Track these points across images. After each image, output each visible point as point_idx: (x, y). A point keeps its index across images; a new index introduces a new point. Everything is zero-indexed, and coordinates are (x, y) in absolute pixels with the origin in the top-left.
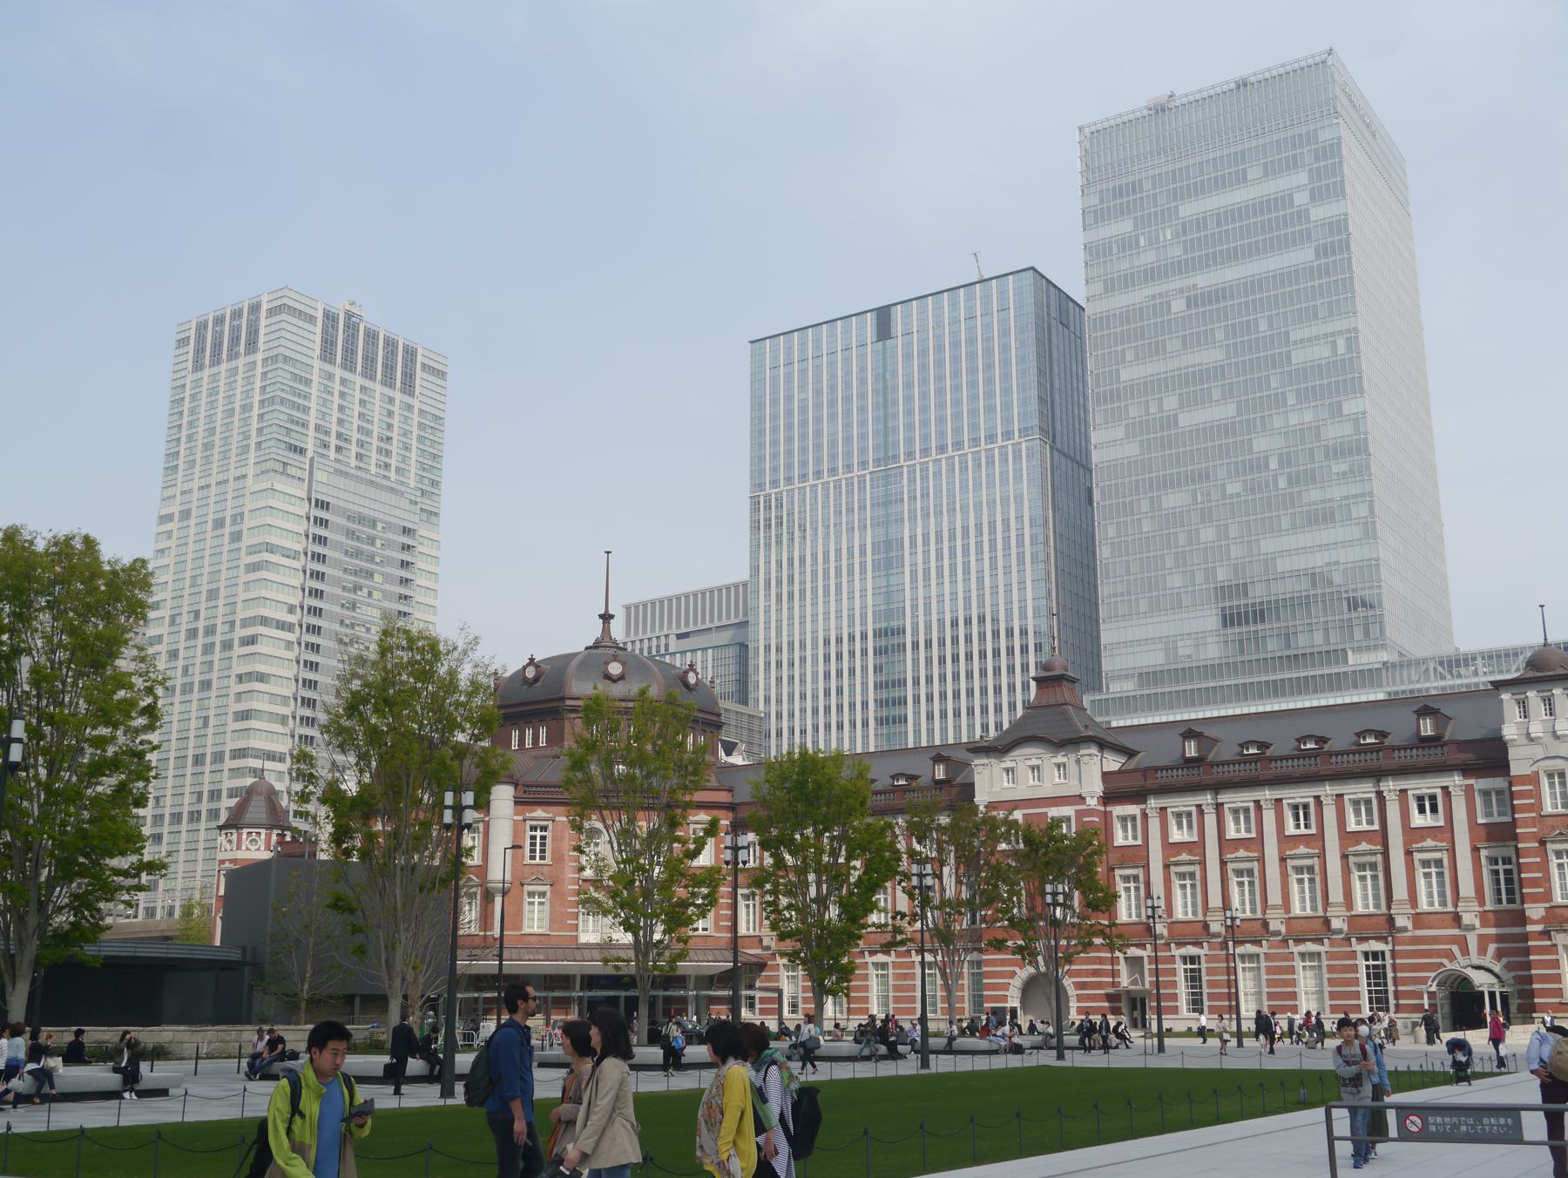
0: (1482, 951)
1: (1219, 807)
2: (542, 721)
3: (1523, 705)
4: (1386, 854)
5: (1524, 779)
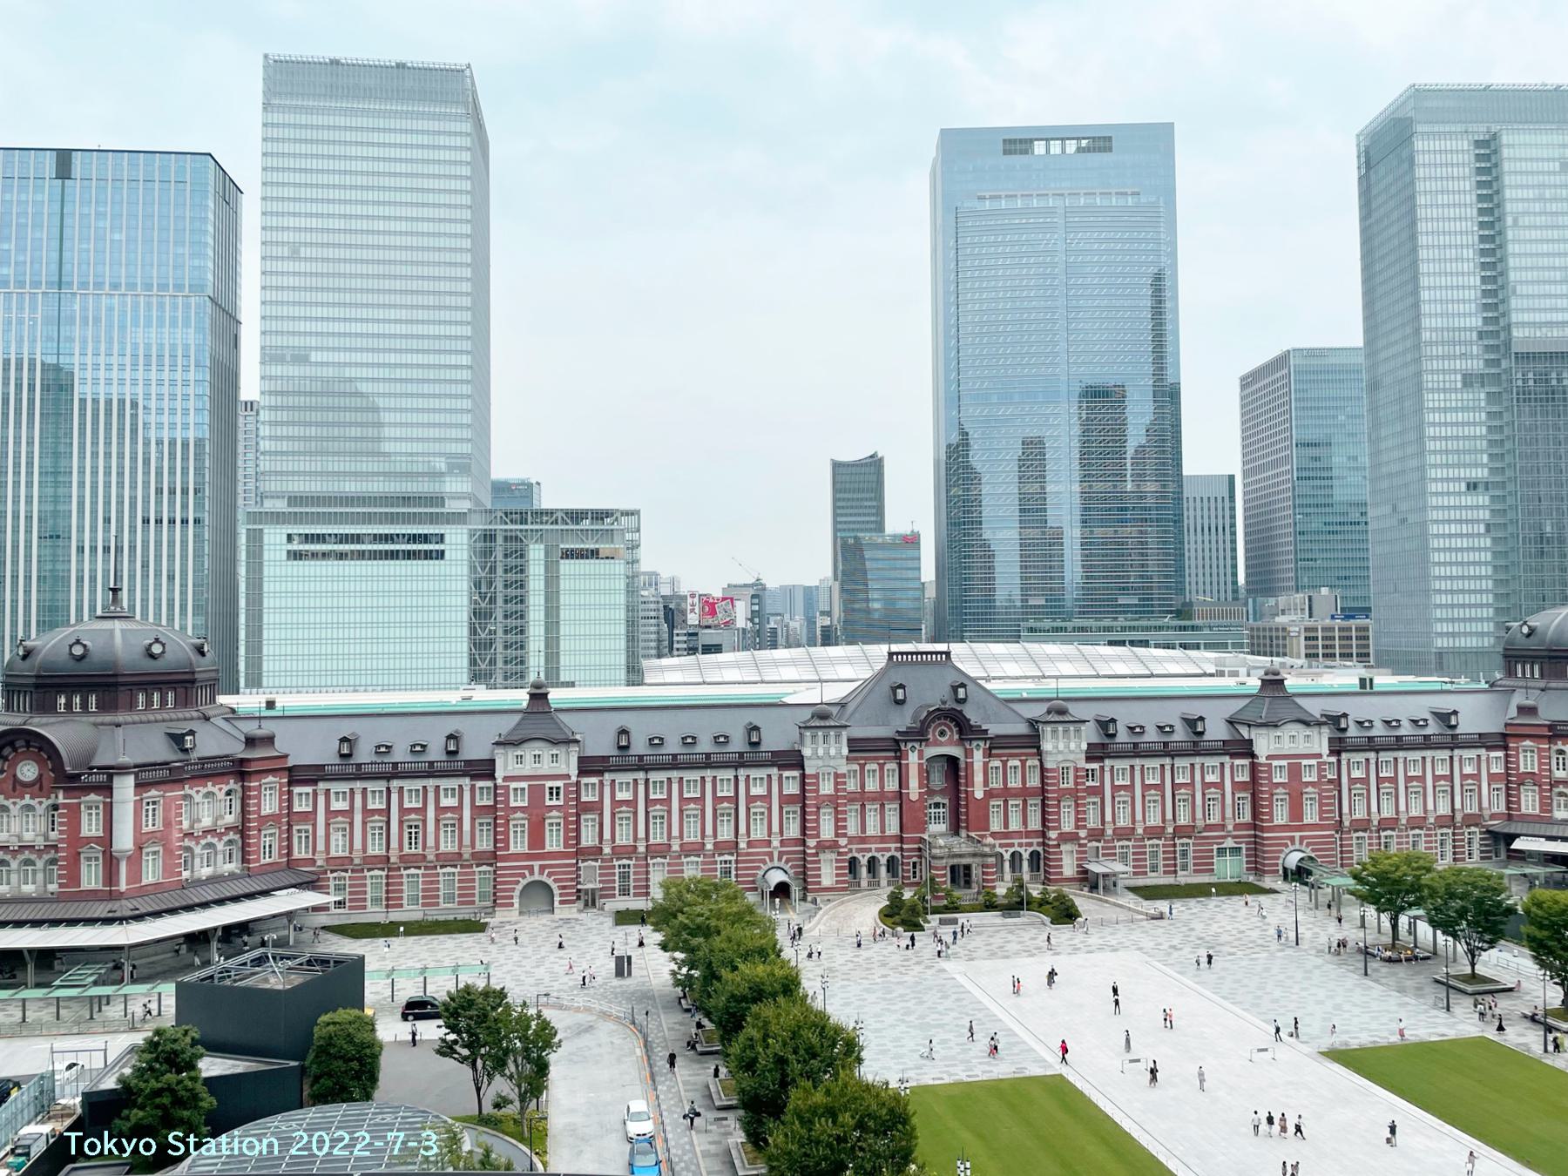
0: (780, 859)
1: (647, 781)
2: (92, 692)
4: (737, 810)
5: (812, 776)
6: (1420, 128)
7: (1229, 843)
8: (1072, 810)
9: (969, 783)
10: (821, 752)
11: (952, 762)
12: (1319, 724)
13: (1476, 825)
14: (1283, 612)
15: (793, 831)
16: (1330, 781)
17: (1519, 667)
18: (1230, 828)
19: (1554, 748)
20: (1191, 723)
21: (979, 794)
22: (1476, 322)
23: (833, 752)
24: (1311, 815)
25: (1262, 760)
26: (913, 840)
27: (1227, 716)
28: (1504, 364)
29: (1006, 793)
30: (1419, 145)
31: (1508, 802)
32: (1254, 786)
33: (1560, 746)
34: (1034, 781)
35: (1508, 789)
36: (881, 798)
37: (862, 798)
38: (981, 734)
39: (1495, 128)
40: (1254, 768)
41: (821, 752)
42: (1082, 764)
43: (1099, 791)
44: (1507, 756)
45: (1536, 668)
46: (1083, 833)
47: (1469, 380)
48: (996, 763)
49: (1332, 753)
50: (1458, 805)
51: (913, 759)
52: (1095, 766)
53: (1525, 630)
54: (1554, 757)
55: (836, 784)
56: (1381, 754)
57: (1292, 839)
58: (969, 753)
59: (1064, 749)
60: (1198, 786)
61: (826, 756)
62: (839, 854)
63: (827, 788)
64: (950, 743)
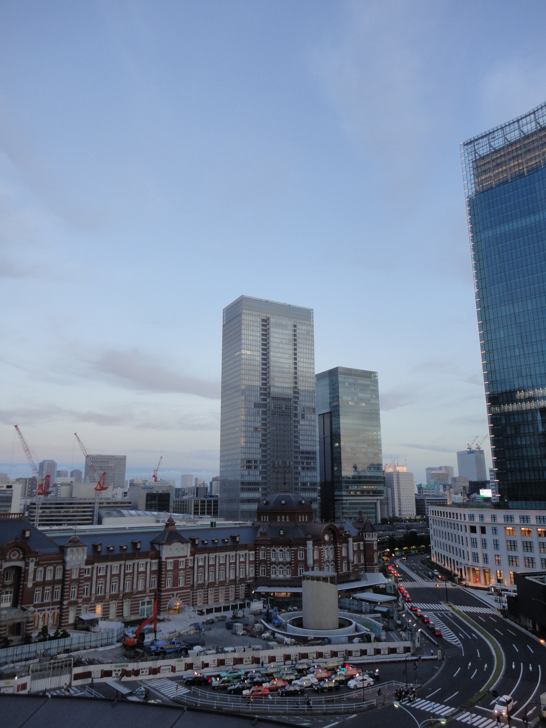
6: (244, 311)
7: (147, 599)
8: (76, 590)
9: (26, 579)
11: (18, 569)
12: (187, 542)
13: (244, 583)
16: (190, 567)
17: (262, 517)
18: (148, 591)
19: (272, 549)
20: (134, 544)
21: (30, 585)
24: (181, 585)
25: (163, 560)
27: (151, 540)
28: (268, 400)
29: (44, 583)
30: (244, 317)
31: (256, 572)
32: (160, 572)
33: (274, 548)
34: (59, 576)
35: (256, 567)
38: (36, 555)
40: (160, 564)
42: (84, 566)
43: (90, 579)
44: (256, 553)
45: (268, 517)
46: (80, 601)
47: (256, 405)
49: (191, 555)
50: (237, 575)
52: (90, 567)
53: (264, 502)
54: (272, 552)
56: (210, 554)
57: (173, 595)
58: (27, 565)
59: (76, 558)
60: (136, 573)
64: (18, 560)
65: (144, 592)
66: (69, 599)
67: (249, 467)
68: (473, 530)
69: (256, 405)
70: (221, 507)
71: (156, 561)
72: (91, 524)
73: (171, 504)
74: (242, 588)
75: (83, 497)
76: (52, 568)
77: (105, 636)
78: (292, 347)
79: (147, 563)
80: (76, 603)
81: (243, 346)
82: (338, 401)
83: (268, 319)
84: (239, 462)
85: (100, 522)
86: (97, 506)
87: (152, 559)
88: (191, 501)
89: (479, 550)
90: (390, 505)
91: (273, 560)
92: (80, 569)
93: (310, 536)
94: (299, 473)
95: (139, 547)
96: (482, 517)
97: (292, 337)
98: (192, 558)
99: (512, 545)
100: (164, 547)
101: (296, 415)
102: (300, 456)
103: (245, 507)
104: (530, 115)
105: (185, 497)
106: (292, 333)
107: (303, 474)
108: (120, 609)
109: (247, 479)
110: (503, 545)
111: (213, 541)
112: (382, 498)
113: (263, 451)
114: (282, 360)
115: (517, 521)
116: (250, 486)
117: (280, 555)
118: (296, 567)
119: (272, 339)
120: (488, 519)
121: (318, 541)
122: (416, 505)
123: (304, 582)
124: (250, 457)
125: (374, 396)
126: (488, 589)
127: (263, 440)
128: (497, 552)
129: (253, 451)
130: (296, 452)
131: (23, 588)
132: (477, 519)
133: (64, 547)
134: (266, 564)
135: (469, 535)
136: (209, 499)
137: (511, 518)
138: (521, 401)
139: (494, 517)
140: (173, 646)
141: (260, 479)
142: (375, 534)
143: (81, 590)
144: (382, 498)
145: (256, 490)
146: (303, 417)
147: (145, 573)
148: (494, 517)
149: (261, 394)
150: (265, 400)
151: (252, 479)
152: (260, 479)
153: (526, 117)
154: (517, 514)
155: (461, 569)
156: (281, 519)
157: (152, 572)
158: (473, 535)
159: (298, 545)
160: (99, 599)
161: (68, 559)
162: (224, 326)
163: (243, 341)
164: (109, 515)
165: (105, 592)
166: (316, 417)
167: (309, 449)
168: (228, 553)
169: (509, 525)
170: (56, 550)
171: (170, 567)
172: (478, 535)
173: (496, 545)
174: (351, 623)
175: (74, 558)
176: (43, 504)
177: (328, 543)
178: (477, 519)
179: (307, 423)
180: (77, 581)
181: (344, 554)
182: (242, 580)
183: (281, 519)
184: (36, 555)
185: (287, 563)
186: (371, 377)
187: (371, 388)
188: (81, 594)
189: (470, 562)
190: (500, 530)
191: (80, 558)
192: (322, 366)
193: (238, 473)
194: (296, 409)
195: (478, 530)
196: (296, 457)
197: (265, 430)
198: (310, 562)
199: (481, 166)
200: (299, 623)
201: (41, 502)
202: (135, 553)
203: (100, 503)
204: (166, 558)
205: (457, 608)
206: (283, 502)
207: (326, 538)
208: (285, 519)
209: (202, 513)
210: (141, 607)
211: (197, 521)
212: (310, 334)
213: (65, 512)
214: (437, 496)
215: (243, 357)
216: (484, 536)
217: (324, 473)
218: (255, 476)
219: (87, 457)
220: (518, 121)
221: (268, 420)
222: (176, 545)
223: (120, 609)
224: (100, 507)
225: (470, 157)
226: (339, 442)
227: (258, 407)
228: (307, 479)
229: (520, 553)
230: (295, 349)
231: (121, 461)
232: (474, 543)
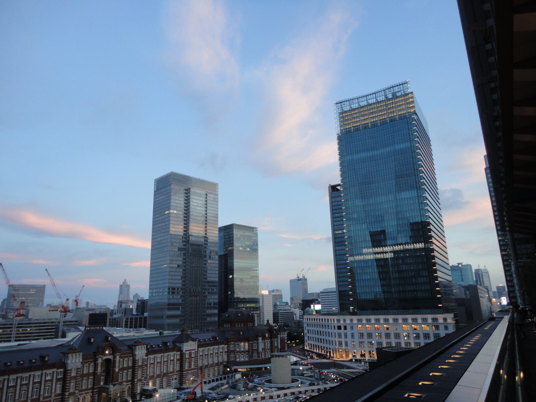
3: (72, 356)
7: (175, 377)
9: (114, 366)
10: (73, 361)
11: (108, 360)
14: (115, 314)
15: (59, 391)
21: (117, 370)
22: (182, 234)
23: (77, 361)
24: (193, 367)
25: (184, 352)
26: (97, 388)
28: (187, 246)
29: (123, 369)
32: (181, 360)
34: (130, 364)
35: (228, 354)
36: (88, 375)
37: (83, 376)
38: (120, 351)
39: (189, 187)
41: (73, 361)
46: (143, 378)
47: (180, 249)
48: (122, 360)
51: (100, 361)
53: (227, 315)
55: (77, 371)
58: (115, 357)
59: (140, 352)
61: (74, 362)
62: (76, 396)
63: (73, 374)
65: (173, 372)
66: (69, 391)
67: (173, 293)
68: (339, 328)
69: (180, 249)
70: (148, 322)
71: (179, 353)
72: (10, 341)
73: (108, 321)
74: (221, 367)
75: (37, 318)
76: (127, 359)
77: (172, 396)
78: (204, 209)
79: (53, 372)
80: (141, 380)
81: (172, 207)
82: (233, 246)
83: (189, 189)
84: (166, 289)
85: (64, 336)
86: (61, 324)
87: (58, 369)
88: (123, 319)
89: (343, 340)
90: (261, 317)
91: (238, 350)
92: (143, 359)
93: (260, 335)
94: (206, 296)
95: (46, 359)
96: (345, 320)
97: (204, 203)
98: (146, 358)
99: (362, 335)
100: (185, 344)
101: (205, 256)
102: (207, 284)
103: (169, 321)
104: (373, 94)
105: (115, 316)
106: (204, 199)
107: (208, 297)
108: (161, 383)
109: (172, 301)
110: (356, 336)
111: (205, 340)
112: (258, 312)
113: (183, 281)
114: (198, 218)
115: (364, 322)
116: (172, 306)
117: (244, 346)
118: (252, 353)
119: (191, 203)
120: (348, 322)
121: (264, 338)
122: (273, 317)
123: (272, 359)
124: (173, 285)
125: (255, 244)
126: (351, 361)
127: (183, 274)
128: (353, 340)
129: (176, 281)
130: (205, 282)
131: (113, 372)
132: (342, 322)
133: (132, 346)
134: (234, 353)
135: (337, 331)
136: (136, 316)
137: (361, 320)
138: (365, 254)
139: (351, 320)
140: (219, 396)
141: (180, 301)
142: (286, 333)
143: (78, 384)
144: (258, 312)
145: (178, 309)
146: (210, 258)
147: (173, 360)
148: (351, 320)
149: (183, 241)
150: (184, 245)
151: (175, 301)
152: (180, 301)
153: (371, 94)
154: (364, 318)
155: (330, 352)
156: (238, 325)
157: (177, 360)
158: (339, 331)
159: (253, 340)
160: (152, 377)
161: (137, 353)
162: (155, 191)
163: (172, 204)
164: (70, 331)
165: (51, 393)
166: (217, 257)
167: (213, 279)
168: (214, 347)
169: (360, 324)
170: (126, 348)
171: (187, 357)
172: (342, 331)
173: (353, 336)
174: (298, 381)
175: (140, 353)
176: (18, 324)
177: (268, 338)
178: (342, 322)
179: (212, 262)
180: (142, 366)
181: (276, 345)
182: (222, 363)
183: (238, 325)
184: (120, 351)
185: (246, 351)
186: (253, 231)
187: (253, 238)
188: (78, 387)
189: (337, 347)
190: (355, 327)
191: (143, 352)
192: (223, 222)
193: (164, 298)
194: (205, 252)
195: (342, 328)
196: (205, 286)
197: (185, 266)
198: (260, 350)
199: (344, 116)
200: (269, 381)
201: (17, 323)
202: (164, 348)
203: (64, 322)
204: (186, 351)
205: (342, 370)
206: (239, 315)
207: (267, 335)
208: (241, 325)
209: (131, 327)
210: (172, 382)
211: (143, 332)
212: (216, 200)
213: (23, 330)
214: (286, 310)
215: (171, 215)
216: (346, 331)
217: (220, 297)
218: (177, 299)
219: (9, 286)
220: (366, 96)
221: (187, 260)
222: (190, 342)
223: (161, 383)
224: (64, 325)
225: (340, 112)
226: (233, 274)
227: (181, 251)
228: (212, 301)
229: (365, 339)
230: (206, 211)
231: (41, 290)
232: (340, 336)
